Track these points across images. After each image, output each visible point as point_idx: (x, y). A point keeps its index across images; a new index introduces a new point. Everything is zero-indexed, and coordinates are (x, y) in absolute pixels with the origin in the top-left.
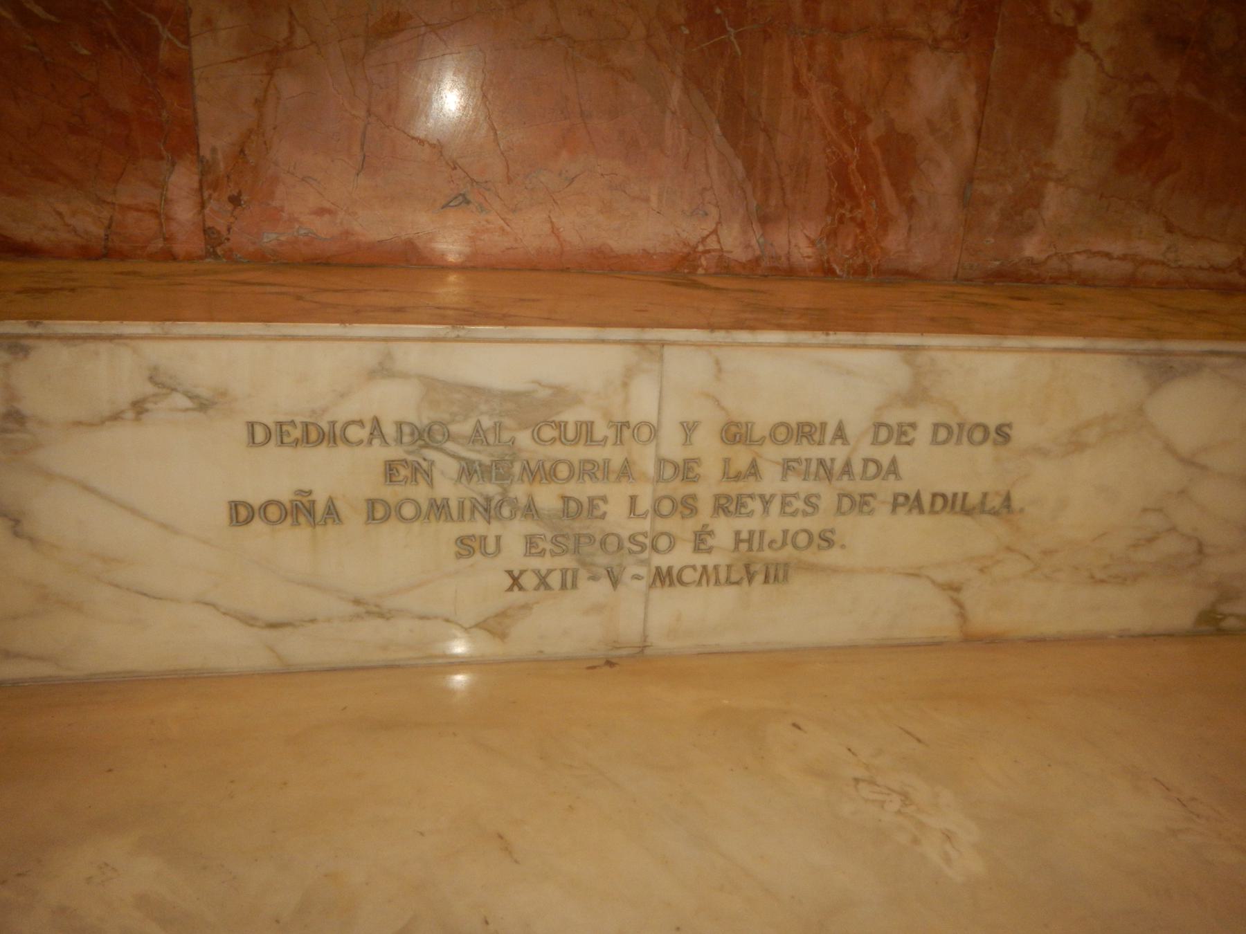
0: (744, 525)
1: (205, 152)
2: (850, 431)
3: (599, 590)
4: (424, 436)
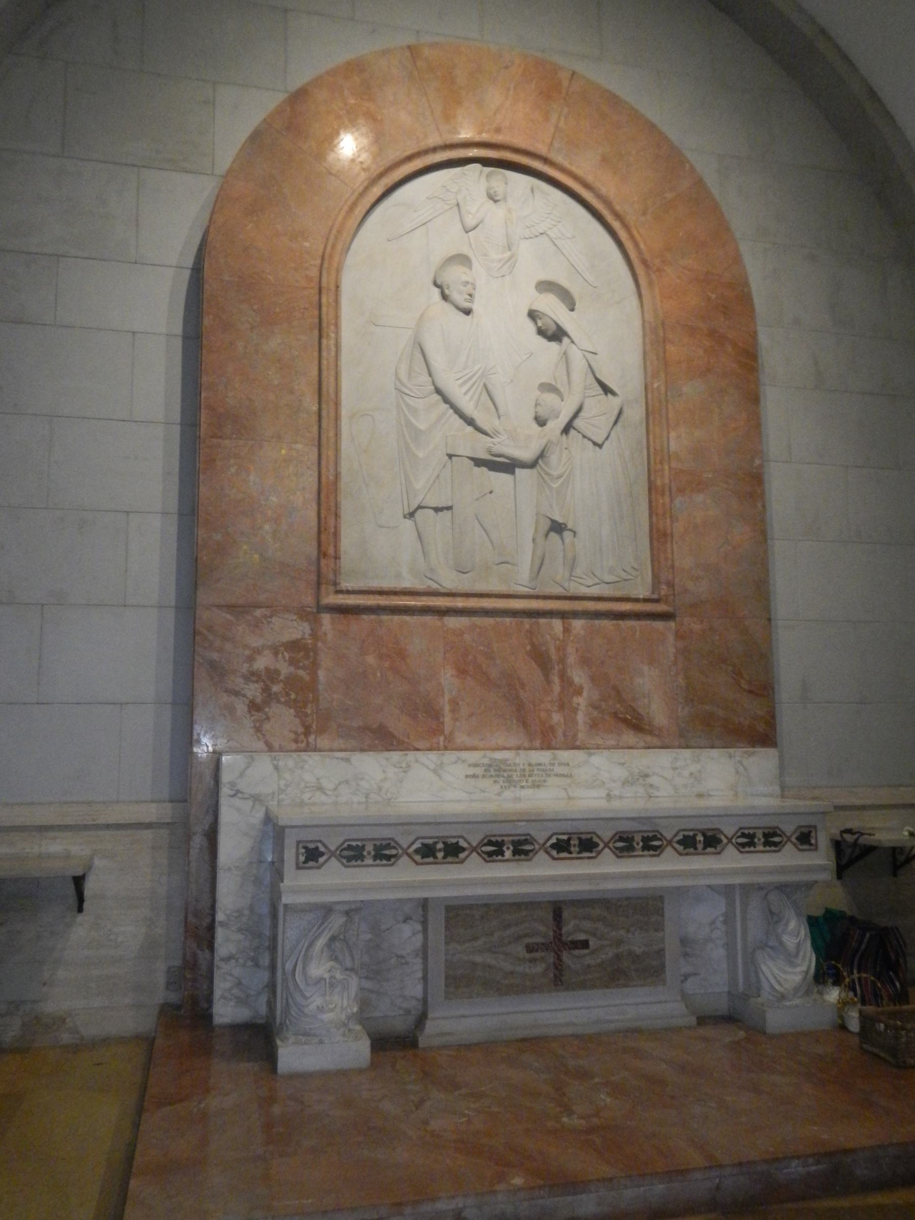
1: (445, 733)
2: (546, 764)
3: (513, 789)
4: (490, 765)
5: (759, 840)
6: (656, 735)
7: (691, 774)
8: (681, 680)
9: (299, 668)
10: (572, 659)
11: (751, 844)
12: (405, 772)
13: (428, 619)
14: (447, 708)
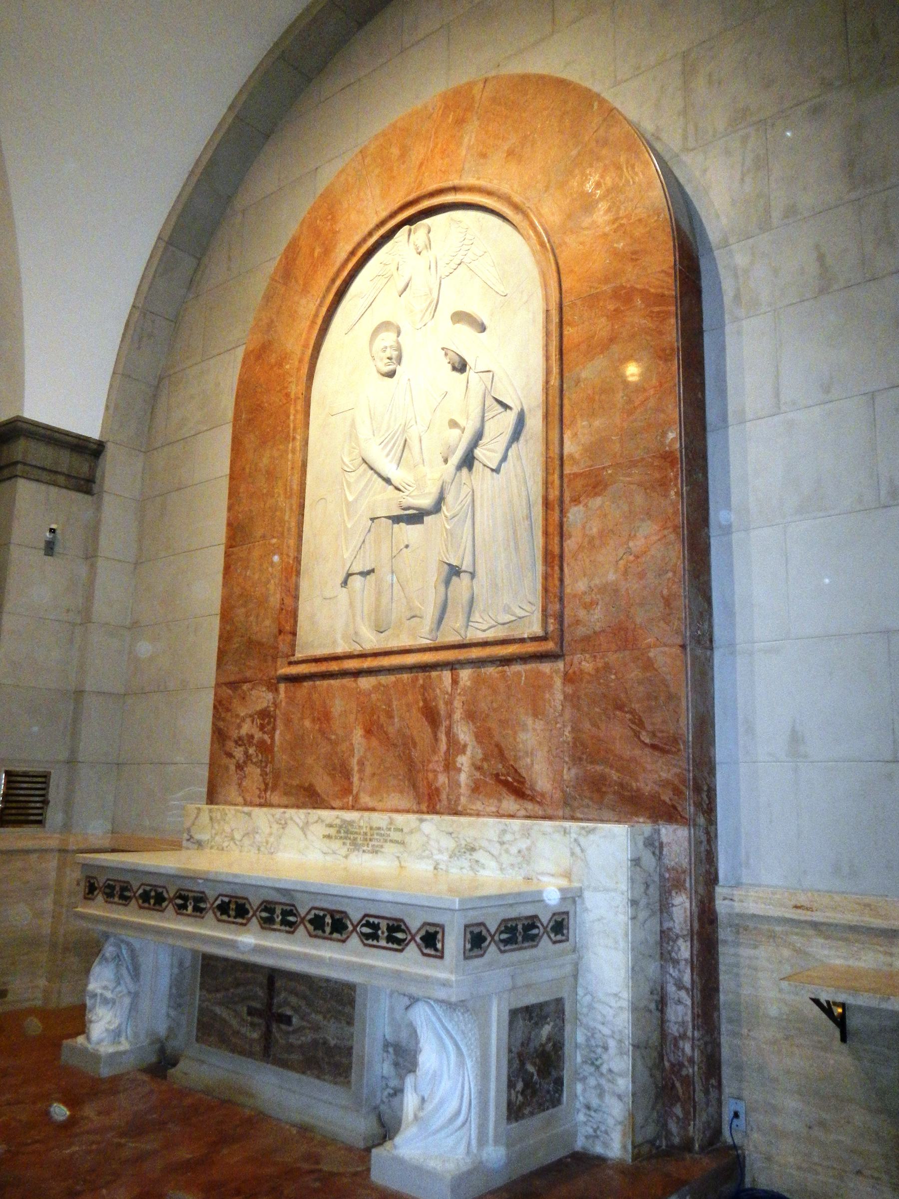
0: (373, 843)
4: (341, 827)
5: (383, 933)
6: (538, 802)
7: (519, 852)
8: (568, 734)
9: (264, 733)
10: (457, 716)
11: (375, 936)
12: (283, 828)
13: (347, 682)
14: (356, 768)
